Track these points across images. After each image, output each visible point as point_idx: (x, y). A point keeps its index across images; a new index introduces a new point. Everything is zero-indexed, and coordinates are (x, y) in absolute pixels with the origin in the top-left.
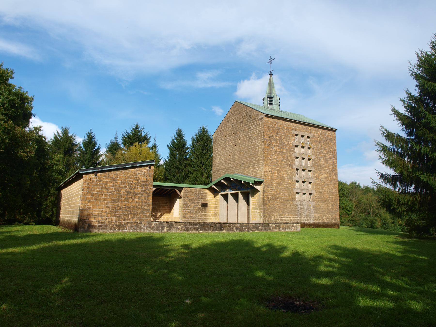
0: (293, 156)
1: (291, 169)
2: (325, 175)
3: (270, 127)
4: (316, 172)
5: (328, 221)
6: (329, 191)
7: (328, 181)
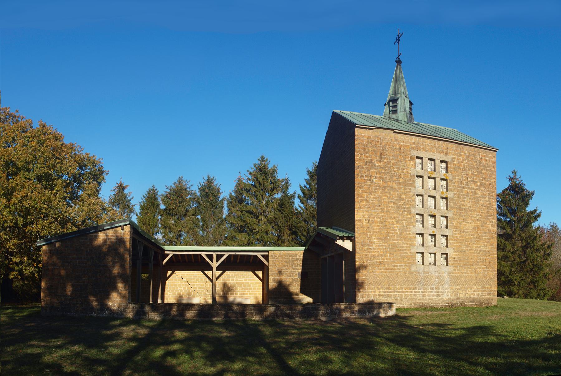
0: (412, 194)
1: (407, 215)
2: (474, 224)
3: (367, 146)
4: (456, 219)
5: (476, 296)
6: (479, 249)
7: (478, 233)
